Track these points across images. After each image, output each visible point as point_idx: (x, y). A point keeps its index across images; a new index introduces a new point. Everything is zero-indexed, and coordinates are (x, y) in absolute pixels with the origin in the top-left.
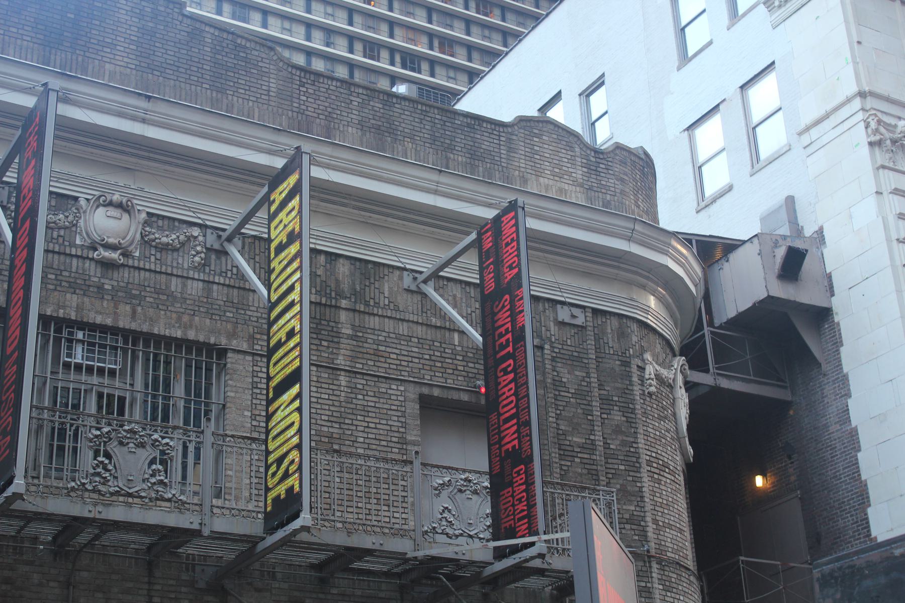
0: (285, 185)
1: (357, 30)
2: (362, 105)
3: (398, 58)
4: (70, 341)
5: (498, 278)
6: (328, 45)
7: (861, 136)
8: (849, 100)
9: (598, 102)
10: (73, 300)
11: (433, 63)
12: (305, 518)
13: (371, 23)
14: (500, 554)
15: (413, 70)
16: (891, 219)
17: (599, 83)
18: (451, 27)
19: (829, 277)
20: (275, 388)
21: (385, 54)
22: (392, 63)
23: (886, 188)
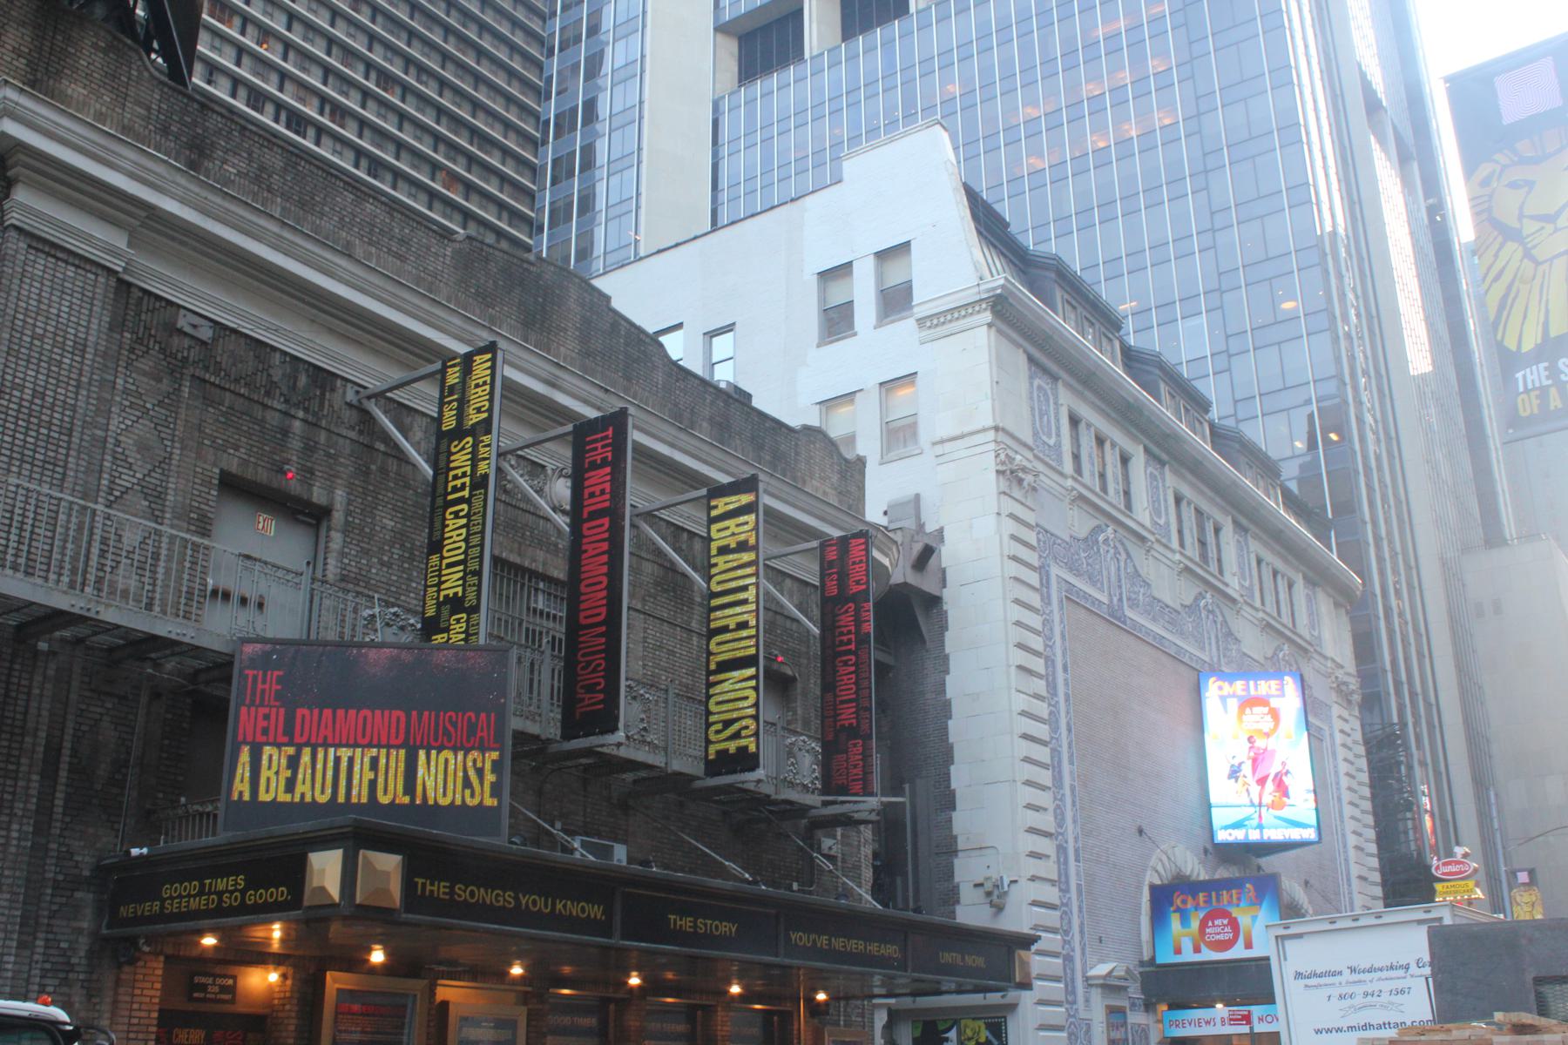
0: (734, 498)
1: (242, 72)
2: (712, 403)
3: (283, 117)
4: (536, 590)
5: (842, 584)
6: (209, 82)
7: (990, 463)
8: (984, 430)
9: (722, 346)
10: (540, 555)
11: (321, 130)
12: (760, 773)
13: (260, 69)
14: (825, 804)
15: (297, 133)
16: (1006, 538)
17: (729, 328)
18: (346, 95)
19: (944, 571)
20: (719, 664)
21: (270, 108)
22: (277, 120)
23: (1005, 512)
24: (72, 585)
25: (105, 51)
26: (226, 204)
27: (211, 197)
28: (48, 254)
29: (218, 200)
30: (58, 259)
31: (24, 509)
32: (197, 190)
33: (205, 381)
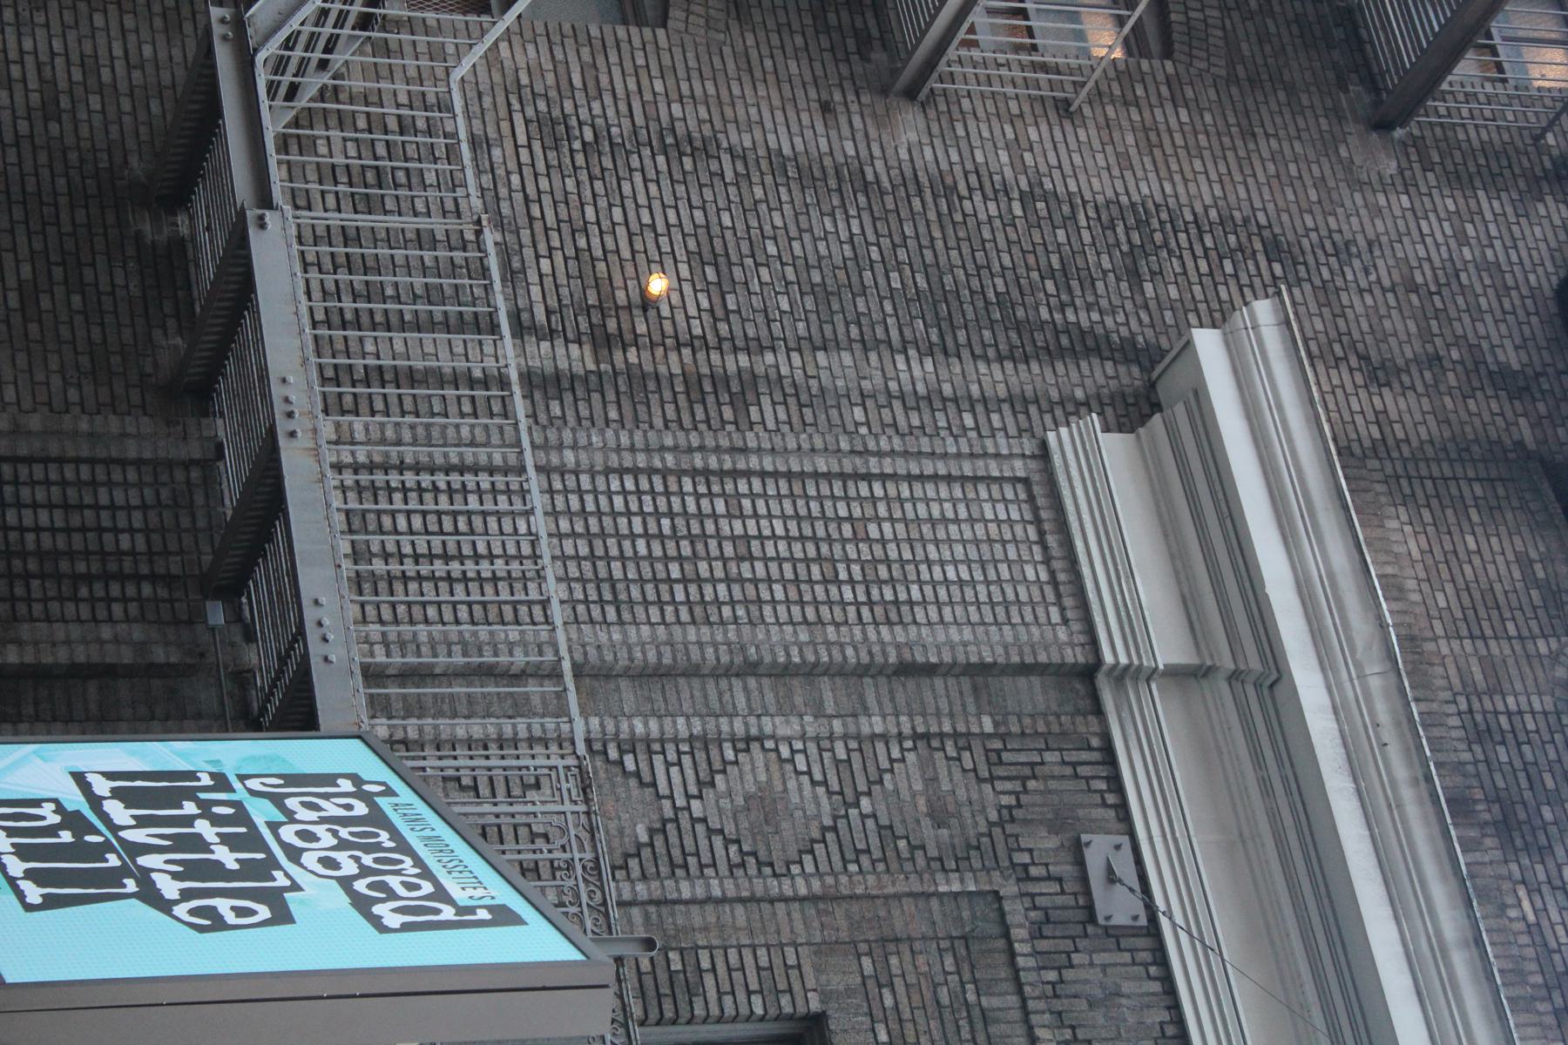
24: (372, 675)
25: (1529, 579)
26: (1407, 794)
27: (1394, 752)
28: (1038, 521)
29: (1401, 773)
30: (1042, 542)
31: (515, 743)
32: (1384, 716)
33: (1006, 935)
